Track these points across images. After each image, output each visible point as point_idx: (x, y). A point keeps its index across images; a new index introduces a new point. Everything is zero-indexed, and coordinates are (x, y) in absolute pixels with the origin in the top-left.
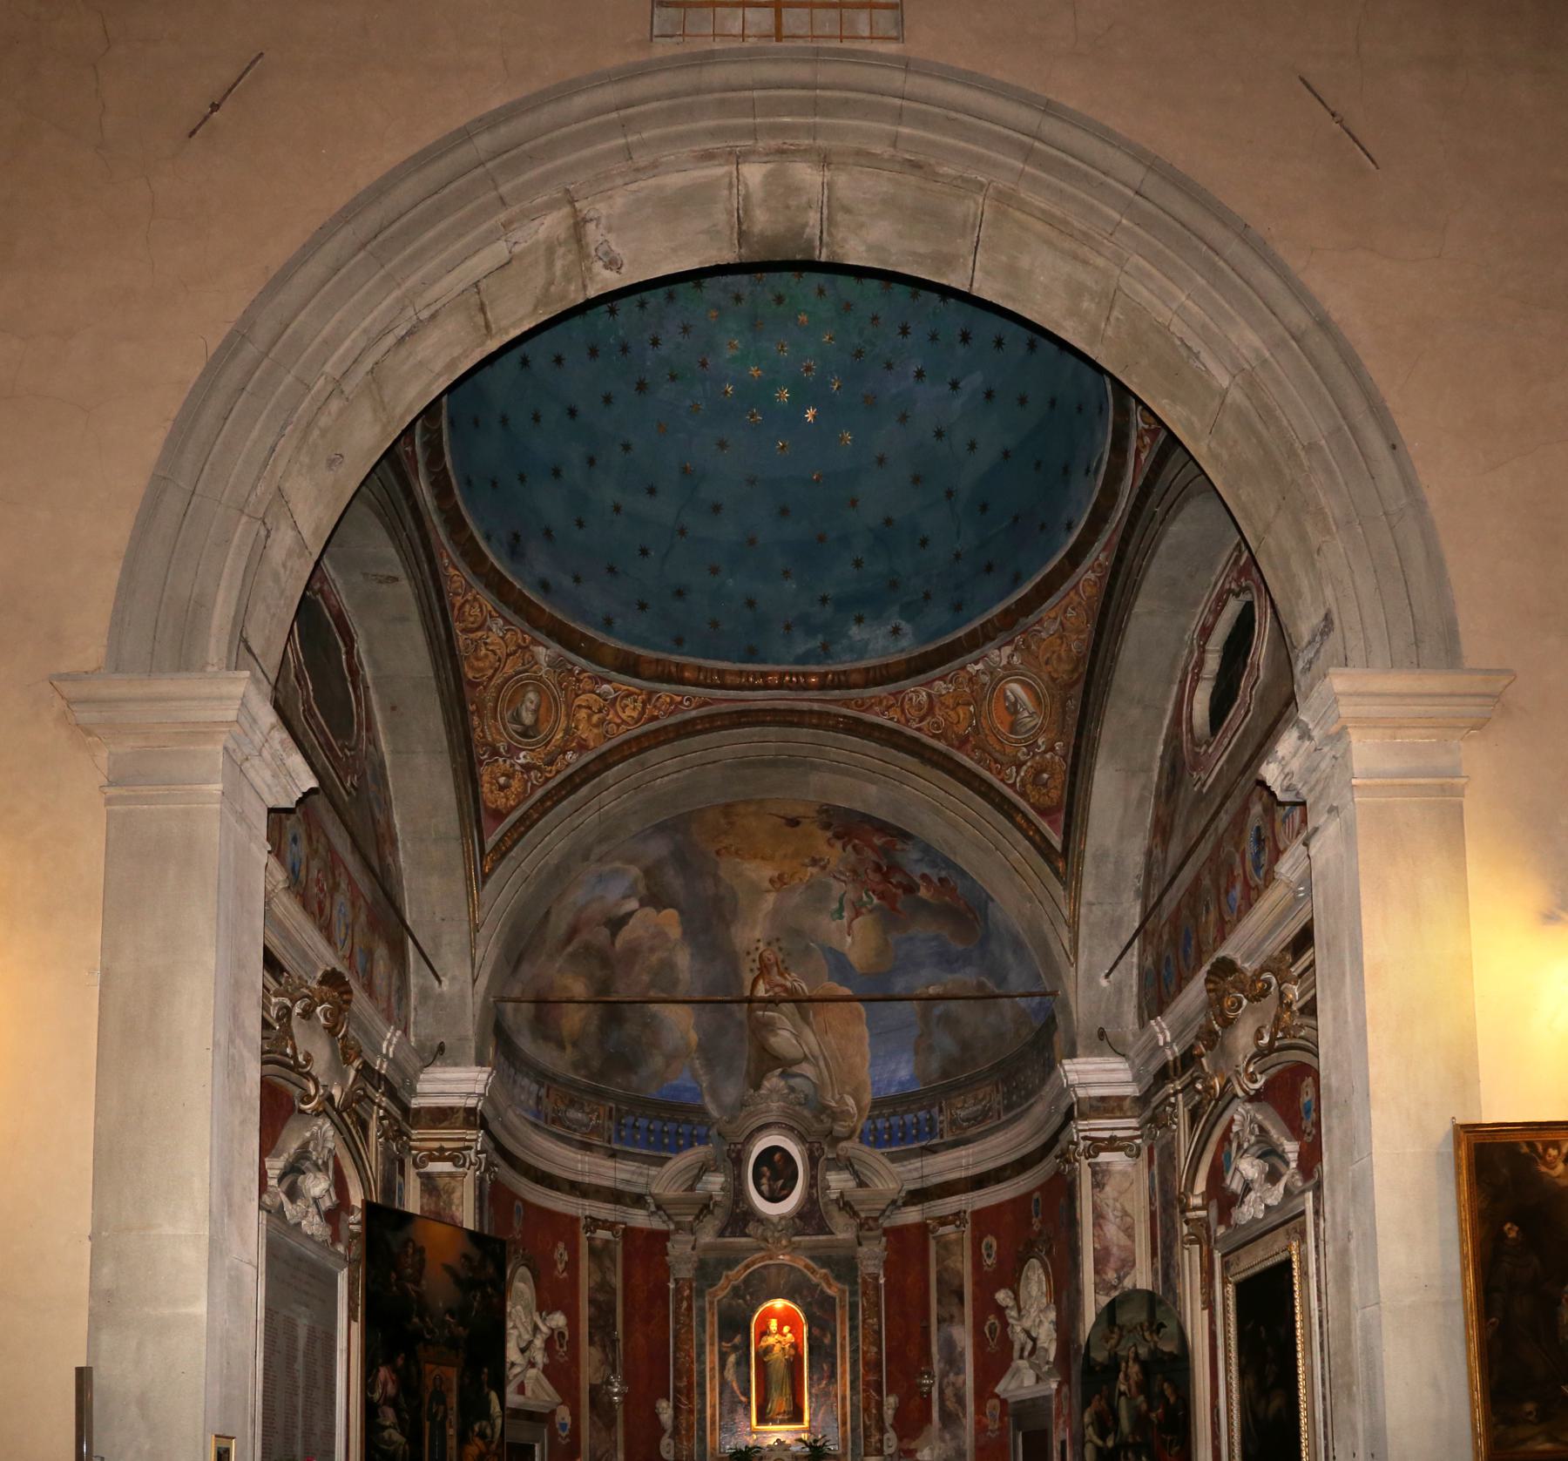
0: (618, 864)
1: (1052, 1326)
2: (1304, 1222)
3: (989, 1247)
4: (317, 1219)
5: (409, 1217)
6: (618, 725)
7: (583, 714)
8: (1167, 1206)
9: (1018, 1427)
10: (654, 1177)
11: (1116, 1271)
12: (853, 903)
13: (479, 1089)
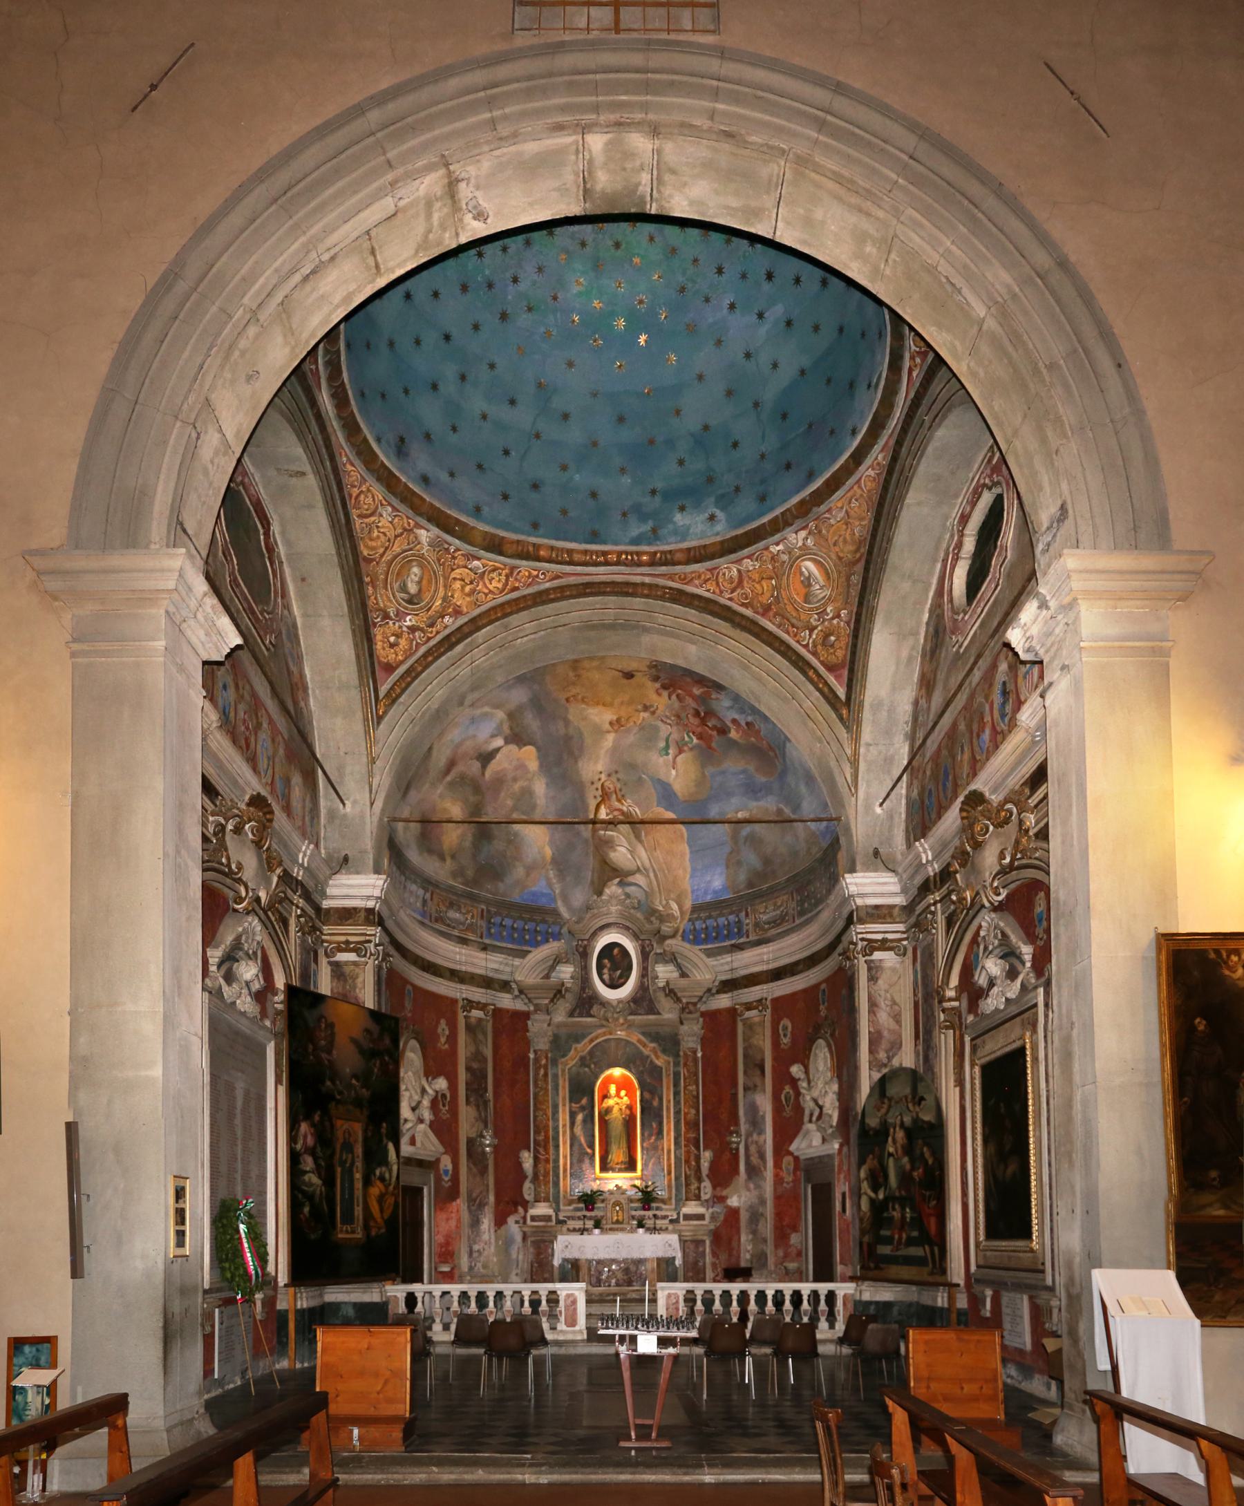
0: (487, 709)
1: (835, 1097)
2: (1036, 1014)
3: (785, 1028)
4: (249, 999)
5: (320, 998)
6: (486, 595)
7: (458, 585)
8: (928, 997)
9: (808, 1180)
10: (517, 967)
11: (887, 1052)
13: (377, 893)
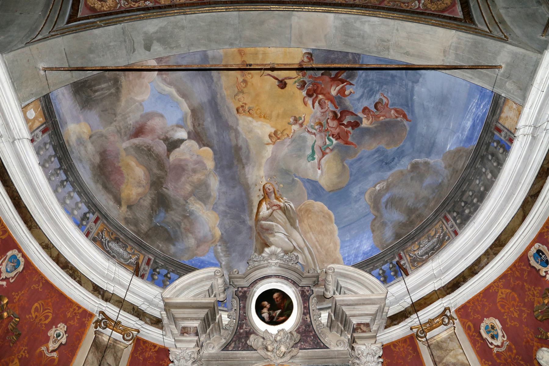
12: (321, 148)
